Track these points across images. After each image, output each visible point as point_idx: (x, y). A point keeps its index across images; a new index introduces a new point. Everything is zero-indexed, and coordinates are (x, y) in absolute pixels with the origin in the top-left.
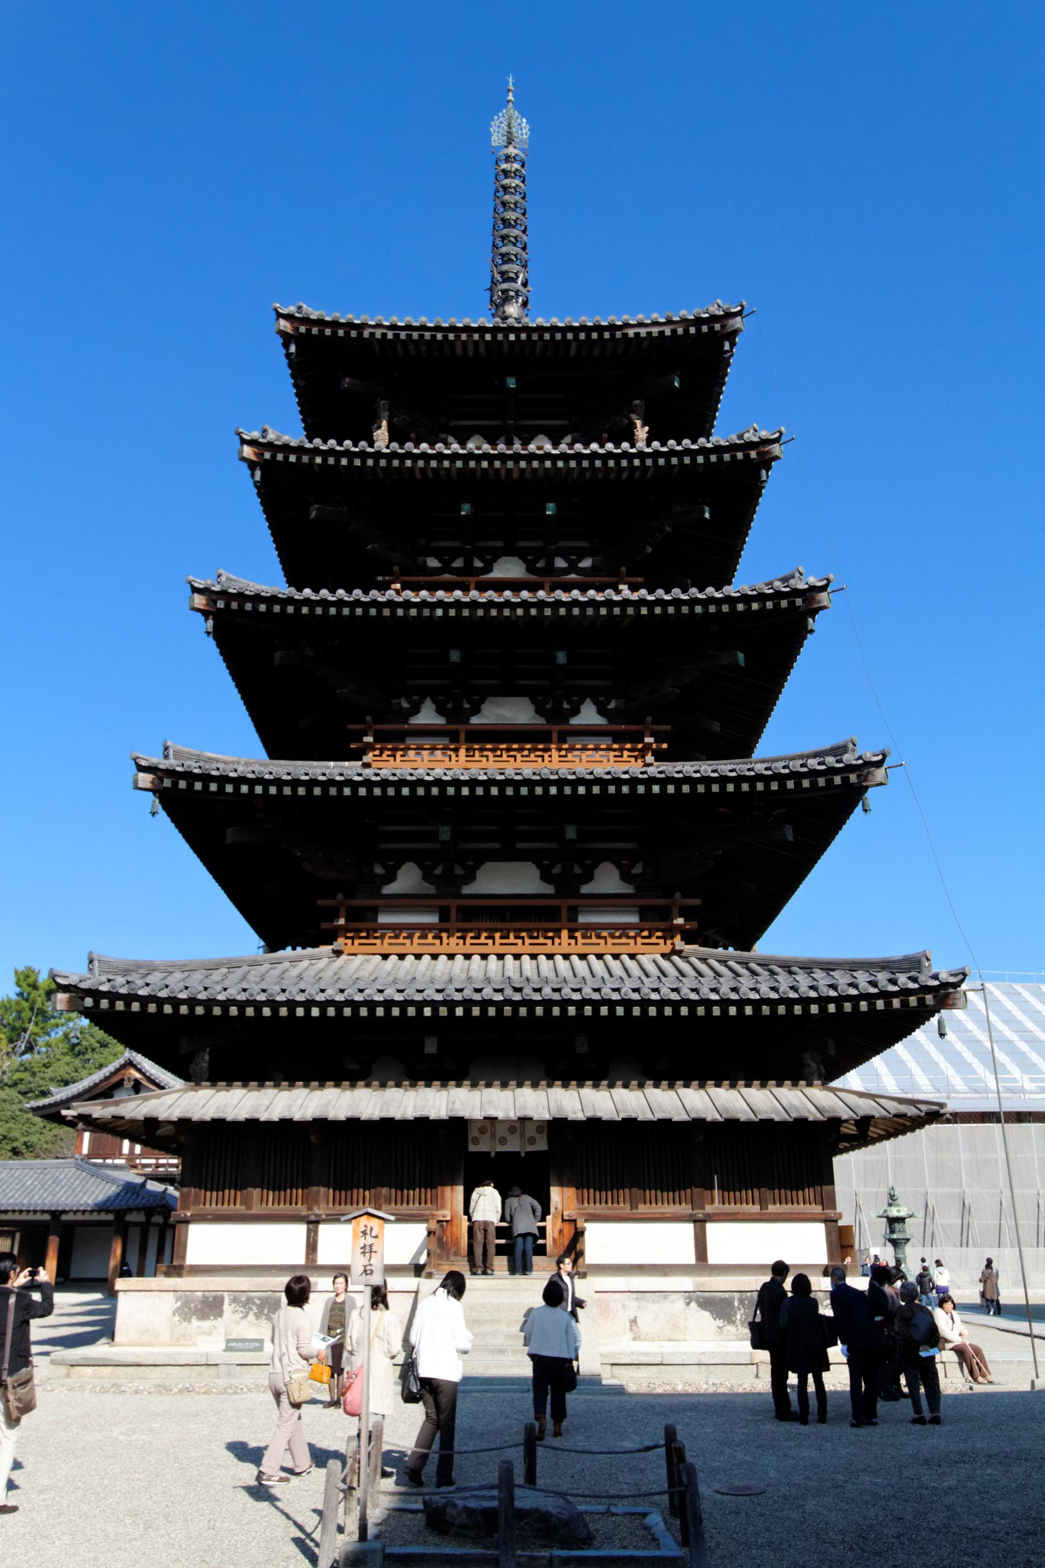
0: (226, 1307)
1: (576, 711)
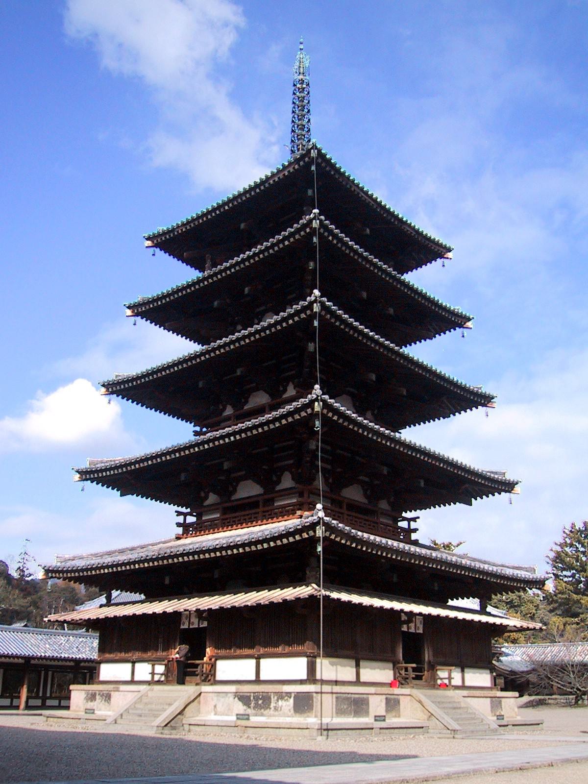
0: (97, 697)
1: (285, 391)
